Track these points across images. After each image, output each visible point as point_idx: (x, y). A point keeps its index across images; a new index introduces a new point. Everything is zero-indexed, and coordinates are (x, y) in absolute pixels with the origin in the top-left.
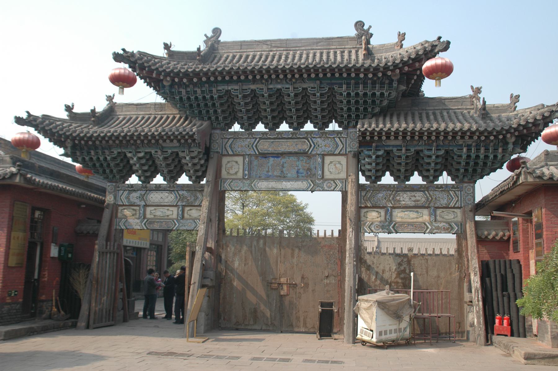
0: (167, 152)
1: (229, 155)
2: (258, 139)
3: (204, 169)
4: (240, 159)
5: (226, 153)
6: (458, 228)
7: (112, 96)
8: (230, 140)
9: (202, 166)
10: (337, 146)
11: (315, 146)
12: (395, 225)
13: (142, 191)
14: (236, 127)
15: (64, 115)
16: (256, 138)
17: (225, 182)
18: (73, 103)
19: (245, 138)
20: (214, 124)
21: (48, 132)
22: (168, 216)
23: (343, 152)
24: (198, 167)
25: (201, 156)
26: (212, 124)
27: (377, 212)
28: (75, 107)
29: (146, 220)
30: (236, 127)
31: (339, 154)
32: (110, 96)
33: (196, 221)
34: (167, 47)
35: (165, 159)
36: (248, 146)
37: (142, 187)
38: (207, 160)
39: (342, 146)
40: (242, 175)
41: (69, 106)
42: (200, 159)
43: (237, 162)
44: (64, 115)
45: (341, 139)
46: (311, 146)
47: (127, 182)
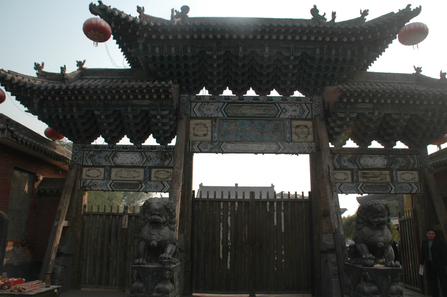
0: (136, 110)
1: (197, 118)
2: (226, 104)
3: (172, 130)
4: (208, 123)
5: (195, 116)
6: (418, 188)
7: (83, 61)
8: (198, 103)
9: (171, 127)
10: (304, 111)
11: (282, 111)
12: (362, 186)
13: (108, 152)
14: (204, 92)
15: (33, 73)
16: (225, 102)
17: (193, 145)
18: (43, 63)
19: (214, 102)
20: (183, 87)
21: (14, 86)
22: (134, 177)
23: (309, 116)
24: (167, 128)
25: (171, 116)
26: (181, 87)
27: (345, 173)
28: (45, 66)
29: (111, 181)
30: (204, 92)
31: (306, 119)
32: (81, 62)
33: (163, 182)
34: (140, 10)
35: (135, 117)
36: (217, 110)
37: (109, 148)
38: (176, 121)
39: (308, 111)
40: (210, 139)
41: (38, 65)
42: (170, 120)
43: (205, 125)
44: (33, 73)
45: (307, 105)
46: (278, 111)
47: (92, 143)
